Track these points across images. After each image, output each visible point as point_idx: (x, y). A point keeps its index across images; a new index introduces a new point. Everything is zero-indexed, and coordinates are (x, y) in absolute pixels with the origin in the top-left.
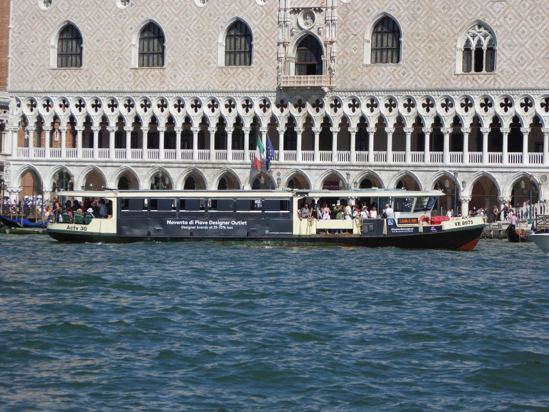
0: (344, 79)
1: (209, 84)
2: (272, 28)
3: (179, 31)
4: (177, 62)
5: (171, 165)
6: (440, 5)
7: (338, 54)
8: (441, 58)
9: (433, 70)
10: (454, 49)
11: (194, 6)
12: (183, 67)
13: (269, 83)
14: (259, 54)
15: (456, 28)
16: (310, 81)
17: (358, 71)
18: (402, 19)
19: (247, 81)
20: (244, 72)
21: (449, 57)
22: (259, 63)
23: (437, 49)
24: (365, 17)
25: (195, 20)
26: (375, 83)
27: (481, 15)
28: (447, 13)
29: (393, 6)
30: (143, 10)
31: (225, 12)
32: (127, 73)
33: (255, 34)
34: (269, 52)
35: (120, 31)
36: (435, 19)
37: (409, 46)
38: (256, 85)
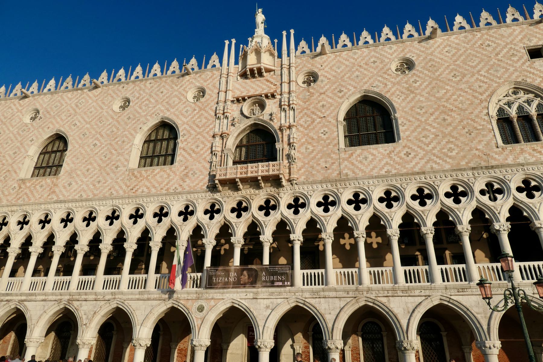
0: (310, 169)
1: (112, 190)
2: (206, 122)
3: (88, 137)
4: (76, 170)
5: (33, 297)
6: (448, 74)
7: (300, 140)
8: (466, 130)
9: (457, 146)
10: (486, 118)
11: (111, 112)
12: (83, 174)
13: (196, 182)
14: (186, 151)
15: (481, 94)
16: (260, 169)
17: (332, 158)
18: (393, 94)
19: (165, 183)
20: (162, 173)
21: (481, 127)
22: (184, 160)
23: (457, 121)
24: (337, 99)
25: (109, 125)
26: (360, 170)
27: (517, 77)
28: (461, 80)
29: (377, 83)
30: (51, 122)
31: (147, 113)
32: (11, 186)
33: (182, 131)
34: (199, 148)
35: (18, 144)
36: (445, 89)
37: (410, 121)
38: (177, 186)
